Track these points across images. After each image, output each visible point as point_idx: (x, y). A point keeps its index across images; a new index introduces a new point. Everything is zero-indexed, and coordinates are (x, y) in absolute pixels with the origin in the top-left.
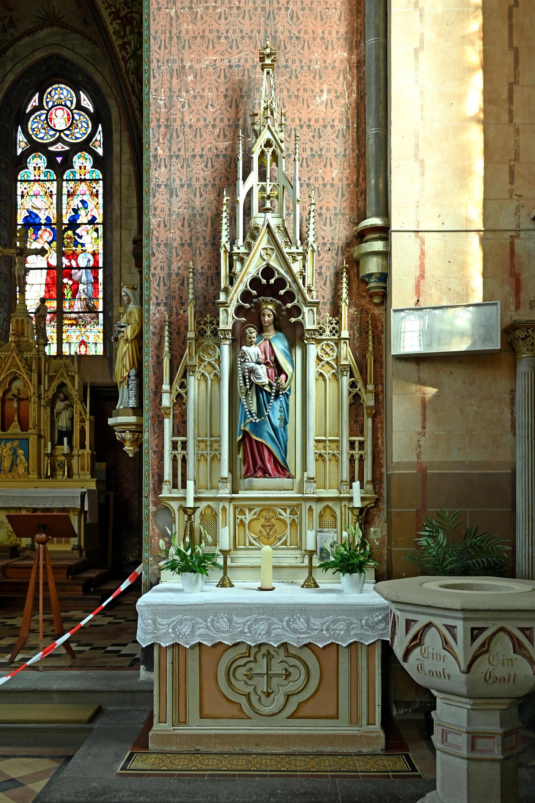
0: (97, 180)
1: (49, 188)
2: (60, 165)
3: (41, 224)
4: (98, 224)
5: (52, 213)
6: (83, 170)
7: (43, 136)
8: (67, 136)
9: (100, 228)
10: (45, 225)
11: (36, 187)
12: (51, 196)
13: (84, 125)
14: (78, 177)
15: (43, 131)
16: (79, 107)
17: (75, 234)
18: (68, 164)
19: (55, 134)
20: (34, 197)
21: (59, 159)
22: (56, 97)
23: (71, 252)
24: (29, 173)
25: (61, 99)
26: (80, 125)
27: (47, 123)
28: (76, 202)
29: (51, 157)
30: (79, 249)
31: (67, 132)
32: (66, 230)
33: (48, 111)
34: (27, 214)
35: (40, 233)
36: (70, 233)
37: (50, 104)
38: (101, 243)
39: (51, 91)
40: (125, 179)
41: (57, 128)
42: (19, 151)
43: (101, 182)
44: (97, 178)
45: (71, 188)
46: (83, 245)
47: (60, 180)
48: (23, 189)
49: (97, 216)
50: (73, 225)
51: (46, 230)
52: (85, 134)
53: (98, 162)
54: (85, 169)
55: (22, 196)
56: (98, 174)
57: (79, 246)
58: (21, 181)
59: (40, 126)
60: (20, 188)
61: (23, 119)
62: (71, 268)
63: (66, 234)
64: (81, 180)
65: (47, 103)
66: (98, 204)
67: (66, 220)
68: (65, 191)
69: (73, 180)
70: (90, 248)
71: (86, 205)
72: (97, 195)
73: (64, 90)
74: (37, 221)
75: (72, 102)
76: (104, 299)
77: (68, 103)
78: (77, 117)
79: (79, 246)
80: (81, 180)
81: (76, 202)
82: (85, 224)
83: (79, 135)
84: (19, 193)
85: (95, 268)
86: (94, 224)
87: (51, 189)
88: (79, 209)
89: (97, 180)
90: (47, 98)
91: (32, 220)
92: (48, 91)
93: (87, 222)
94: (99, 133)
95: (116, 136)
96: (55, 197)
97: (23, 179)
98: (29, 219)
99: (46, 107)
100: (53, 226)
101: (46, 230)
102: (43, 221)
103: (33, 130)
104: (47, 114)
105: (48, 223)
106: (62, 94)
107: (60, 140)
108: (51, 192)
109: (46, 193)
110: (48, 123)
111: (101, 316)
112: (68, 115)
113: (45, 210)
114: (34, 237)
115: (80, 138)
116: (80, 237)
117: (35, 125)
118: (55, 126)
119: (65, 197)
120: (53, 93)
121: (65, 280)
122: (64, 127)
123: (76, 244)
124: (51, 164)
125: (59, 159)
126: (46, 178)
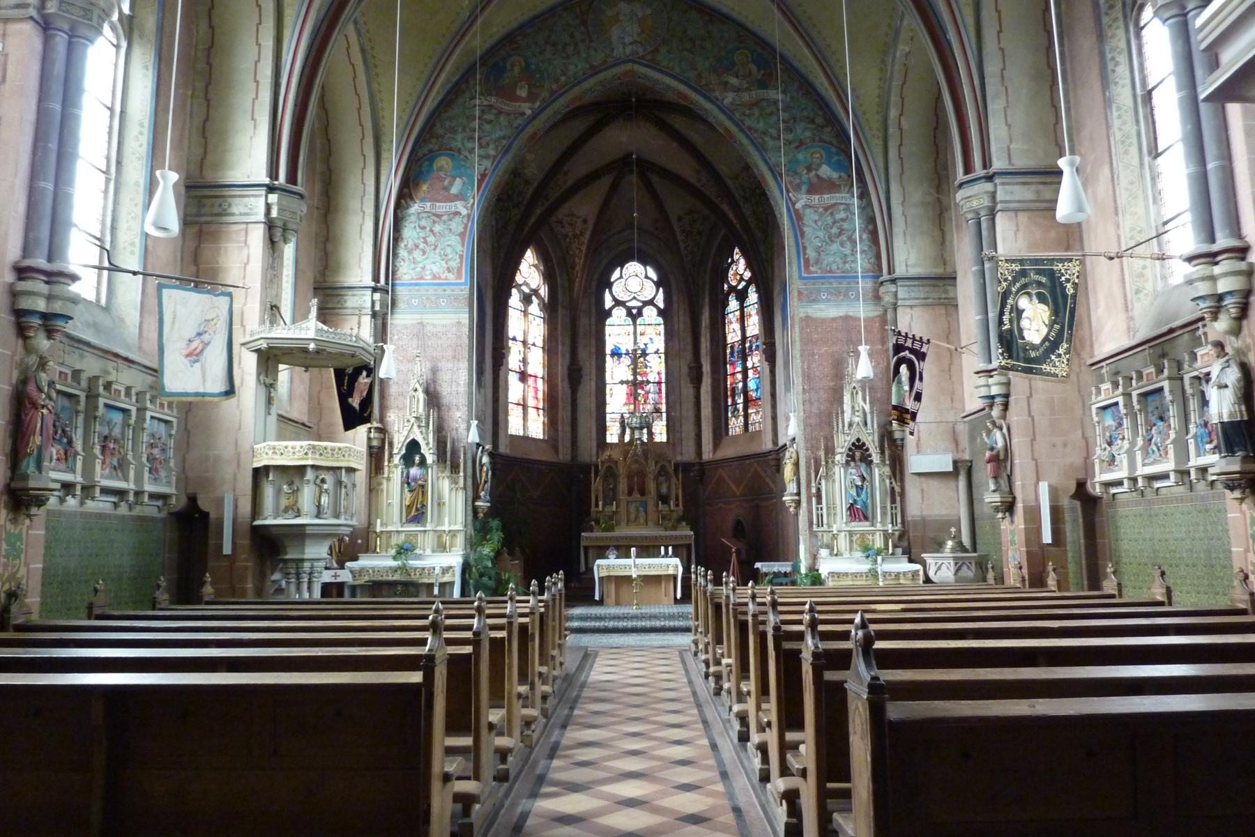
7: (622, 297)
9: (663, 356)
16: (647, 277)
18: (640, 314)
21: (634, 311)
29: (629, 310)
30: (648, 370)
38: (663, 365)
40: (682, 326)
50: (644, 354)
53: (661, 313)
56: (660, 320)
60: (607, 328)
61: (609, 285)
62: (642, 382)
70: (656, 369)
76: (667, 403)
85: (659, 383)
95: (675, 298)
105: (627, 354)
111: (664, 415)
113: (626, 345)
121: (639, 391)
123: (646, 367)
125: (634, 311)
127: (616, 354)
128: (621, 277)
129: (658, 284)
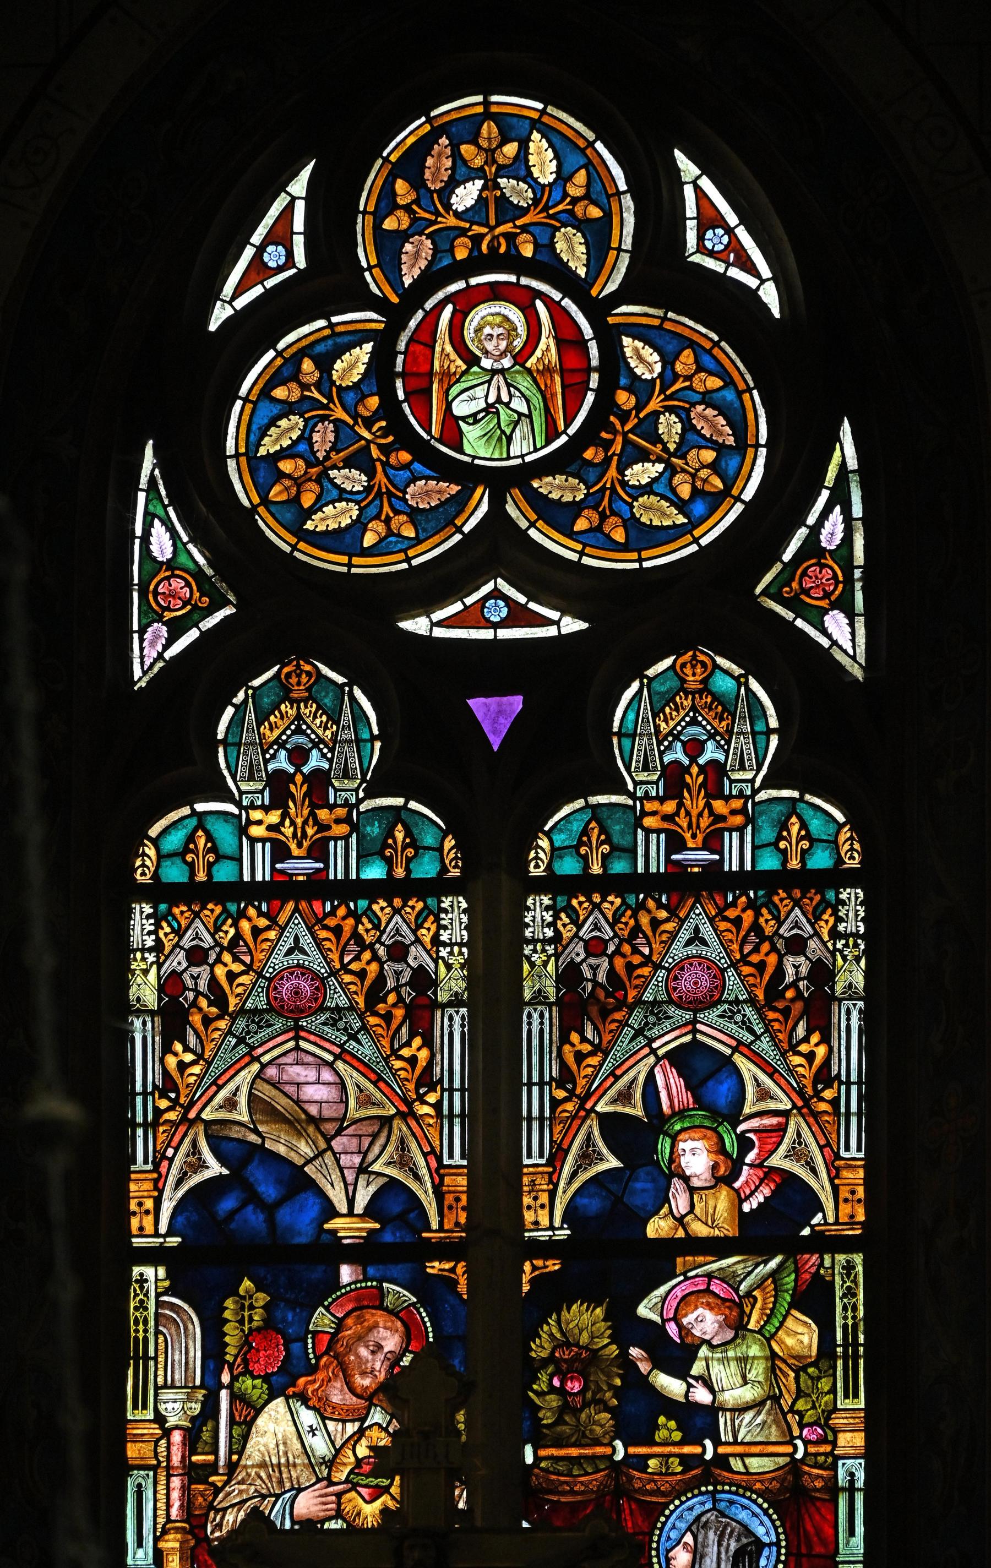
0: (815, 885)
1: (398, 952)
2: (491, 762)
3: (338, 1251)
4: (825, 1243)
5: (434, 1165)
6: (694, 803)
8: (558, 516)
9: (848, 1273)
10: (357, 1254)
11: (293, 945)
12: (421, 1011)
13: (707, 420)
14: (652, 856)
15: (353, 480)
16: (663, 272)
17: (627, 1328)
18: (567, 747)
19: (460, 503)
20: (273, 1026)
22: (466, 196)
23: (593, 1480)
24: (234, 825)
25: (507, 210)
26: (670, 427)
27: (390, 407)
28: (642, 1070)
29: (424, 692)
31: (554, 487)
32: (552, 1295)
33: (396, 317)
34: (215, 1168)
35: (322, 1320)
36: (585, 1320)
37: (415, 260)
39: (423, 146)
41: (477, 445)
42: (150, 651)
43: (853, 904)
44: (821, 860)
45: (595, 947)
46: (699, 1421)
47: (494, 878)
48: (178, 961)
49: (821, 1186)
50: (615, 1250)
51: (377, 1300)
52: (716, 501)
53: (829, 733)
54: (714, 789)
55: (173, 1019)
56: (826, 829)
57: (668, 1428)
58: (159, 892)
59: (323, 438)
61: (183, 388)
63: (551, 1326)
64: (680, 886)
65: (389, 247)
66: (824, 1076)
67: (544, 1219)
68: (540, 975)
69: (608, 884)
71: (722, 1092)
72: (818, 1009)
73: (537, 142)
74: (299, 1220)
75: (599, 238)
77: (572, 250)
78: (644, 360)
79: (668, 1428)
80: (680, 886)
81: (642, 1070)
82: (718, 1247)
83: (673, 509)
84: (145, 989)
86: (794, 1248)
87: (417, 956)
88: (658, 1121)
89: (815, 885)
90: (387, 202)
91: (254, 1218)
92: (393, 149)
93: (728, 1229)
94: (840, 497)
96: (453, 1027)
97: (174, 873)
98: (227, 1204)
99: (374, 283)
100: (435, 1267)
101: (377, 1300)
102: (348, 1228)
103: (264, 469)
104: (384, 346)
106: (520, 168)
107: (496, 549)
108: (423, 980)
109: (375, 993)
110: (399, 421)
112: (569, 339)
114: (272, 1358)
115: (672, 534)
116: (678, 1357)
117: (290, 428)
118: (454, 438)
119: (537, 1025)
120: (438, 165)
122: (524, 448)
124: (427, 751)
125: (496, 714)
126: (375, 872)
127: (256, 1248)
128: (328, 281)
129: (804, 375)
